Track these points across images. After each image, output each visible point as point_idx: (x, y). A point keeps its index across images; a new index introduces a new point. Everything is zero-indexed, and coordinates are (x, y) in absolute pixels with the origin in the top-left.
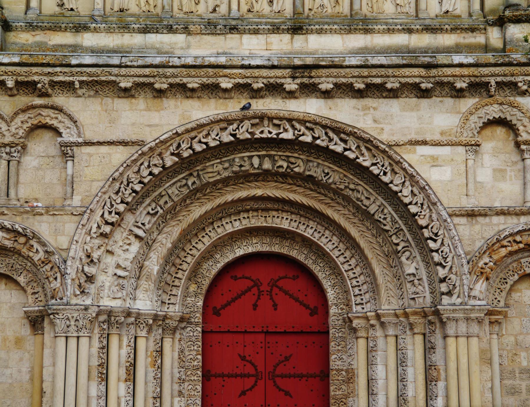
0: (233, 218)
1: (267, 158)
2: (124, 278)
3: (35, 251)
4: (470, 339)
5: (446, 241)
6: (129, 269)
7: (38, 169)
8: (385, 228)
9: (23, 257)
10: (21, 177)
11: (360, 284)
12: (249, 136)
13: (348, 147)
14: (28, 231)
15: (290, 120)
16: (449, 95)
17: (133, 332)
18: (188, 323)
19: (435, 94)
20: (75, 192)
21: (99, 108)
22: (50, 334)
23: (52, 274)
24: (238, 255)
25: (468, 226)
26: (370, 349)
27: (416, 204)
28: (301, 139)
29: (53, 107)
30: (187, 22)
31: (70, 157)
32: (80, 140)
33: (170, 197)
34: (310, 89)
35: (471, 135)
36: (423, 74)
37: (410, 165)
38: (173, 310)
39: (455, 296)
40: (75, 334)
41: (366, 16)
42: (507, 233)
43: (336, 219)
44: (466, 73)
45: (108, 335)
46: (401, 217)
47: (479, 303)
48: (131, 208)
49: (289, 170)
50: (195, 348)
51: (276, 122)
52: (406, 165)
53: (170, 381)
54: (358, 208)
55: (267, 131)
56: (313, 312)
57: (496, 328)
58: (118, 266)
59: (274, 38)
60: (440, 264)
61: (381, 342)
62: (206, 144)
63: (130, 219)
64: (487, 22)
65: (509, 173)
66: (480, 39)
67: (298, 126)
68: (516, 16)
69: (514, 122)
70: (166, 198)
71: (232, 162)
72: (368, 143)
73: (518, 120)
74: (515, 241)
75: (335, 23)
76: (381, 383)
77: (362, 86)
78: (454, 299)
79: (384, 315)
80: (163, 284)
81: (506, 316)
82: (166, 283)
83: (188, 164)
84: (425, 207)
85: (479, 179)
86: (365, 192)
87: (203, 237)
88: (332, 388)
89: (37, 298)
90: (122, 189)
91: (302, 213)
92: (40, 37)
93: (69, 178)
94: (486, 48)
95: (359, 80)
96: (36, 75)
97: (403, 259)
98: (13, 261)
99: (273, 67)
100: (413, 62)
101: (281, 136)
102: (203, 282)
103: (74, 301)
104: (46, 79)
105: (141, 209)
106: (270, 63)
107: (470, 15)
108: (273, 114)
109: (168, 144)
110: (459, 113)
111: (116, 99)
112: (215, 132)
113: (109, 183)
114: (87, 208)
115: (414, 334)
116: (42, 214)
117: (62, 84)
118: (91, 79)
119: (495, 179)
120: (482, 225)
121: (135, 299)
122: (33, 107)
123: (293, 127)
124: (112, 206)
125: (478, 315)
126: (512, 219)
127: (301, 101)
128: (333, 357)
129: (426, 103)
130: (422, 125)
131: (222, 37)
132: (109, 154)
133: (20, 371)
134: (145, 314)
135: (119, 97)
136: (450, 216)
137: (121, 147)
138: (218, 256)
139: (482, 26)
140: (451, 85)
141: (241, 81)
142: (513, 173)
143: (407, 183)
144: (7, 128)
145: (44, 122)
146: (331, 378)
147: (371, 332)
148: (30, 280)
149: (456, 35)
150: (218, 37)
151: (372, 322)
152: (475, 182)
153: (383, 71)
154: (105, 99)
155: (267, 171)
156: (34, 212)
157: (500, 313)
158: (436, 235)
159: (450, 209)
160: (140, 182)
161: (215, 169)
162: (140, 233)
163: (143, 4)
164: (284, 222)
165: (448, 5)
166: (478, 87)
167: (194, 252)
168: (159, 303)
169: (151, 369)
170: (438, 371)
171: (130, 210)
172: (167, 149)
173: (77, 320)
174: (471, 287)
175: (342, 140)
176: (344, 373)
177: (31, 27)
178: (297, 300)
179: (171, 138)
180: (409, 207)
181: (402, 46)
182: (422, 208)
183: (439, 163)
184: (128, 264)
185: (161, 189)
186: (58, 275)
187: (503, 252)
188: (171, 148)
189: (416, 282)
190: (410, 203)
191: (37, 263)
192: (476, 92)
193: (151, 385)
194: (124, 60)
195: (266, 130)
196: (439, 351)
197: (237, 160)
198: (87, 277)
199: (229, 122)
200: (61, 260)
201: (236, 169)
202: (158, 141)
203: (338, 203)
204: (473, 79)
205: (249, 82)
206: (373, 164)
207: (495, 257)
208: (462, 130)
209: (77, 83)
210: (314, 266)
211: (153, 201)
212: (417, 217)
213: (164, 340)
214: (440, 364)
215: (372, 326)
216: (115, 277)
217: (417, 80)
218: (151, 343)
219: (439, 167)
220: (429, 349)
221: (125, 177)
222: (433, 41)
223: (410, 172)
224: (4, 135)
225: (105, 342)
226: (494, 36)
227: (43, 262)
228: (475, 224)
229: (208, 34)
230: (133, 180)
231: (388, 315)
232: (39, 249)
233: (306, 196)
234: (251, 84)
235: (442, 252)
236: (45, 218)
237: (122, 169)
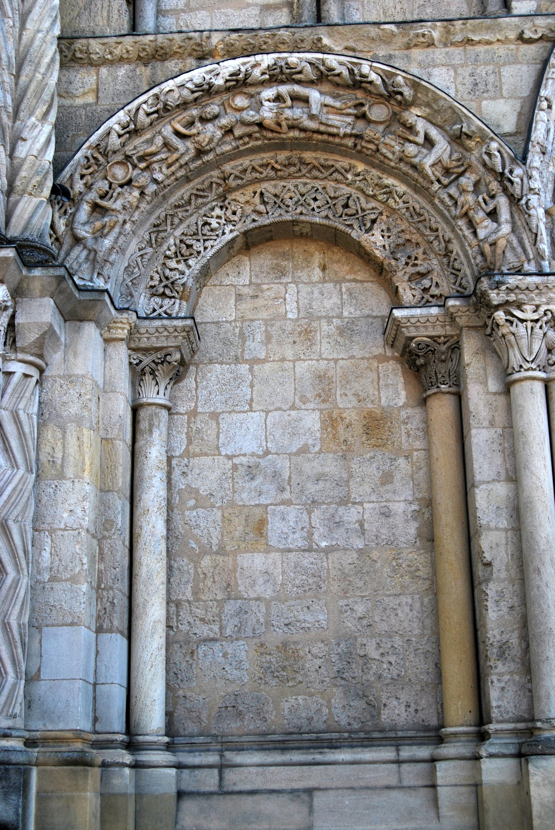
3: (420, 139)
14: (400, 79)
22: (485, 383)
23: (480, 199)
89: (425, 290)
98: (346, 190)
116: (431, 44)
133: (386, 514)
148: (400, 241)
186: (502, 202)
191: (429, 172)
227: (447, 172)
232: (434, 133)
236: (439, 54)
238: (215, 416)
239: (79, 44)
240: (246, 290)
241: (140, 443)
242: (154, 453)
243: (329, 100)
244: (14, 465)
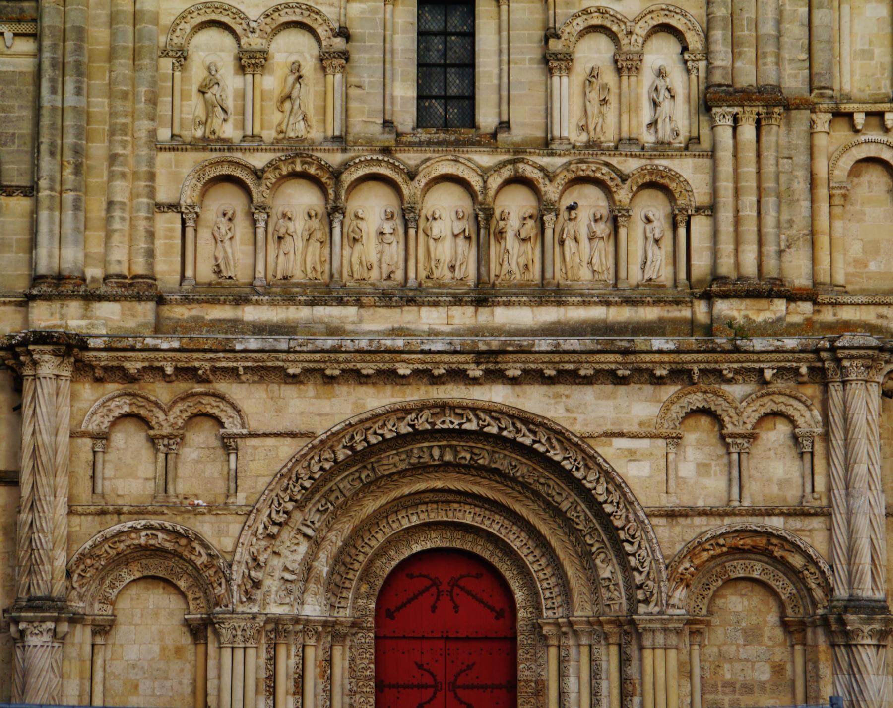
0: (410, 511)
1: (448, 449)
2: (291, 581)
3: (197, 554)
4: (668, 651)
5: (644, 544)
6: (297, 571)
7: (197, 461)
8: (578, 527)
9: (184, 560)
10: (179, 471)
11: (551, 586)
12: (429, 427)
13: (537, 439)
15: (474, 409)
17: (301, 640)
18: (359, 628)
20: (239, 489)
21: (264, 395)
24: (414, 551)
25: (667, 528)
26: (562, 659)
27: (612, 502)
28: (486, 430)
29: (214, 395)
30: (359, 293)
31: (234, 449)
32: (245, 431)
33: (341, 492)
34: (496, 376)
35: (672, 426)
37: (605, 460)
38: (343, 615)
39: (652, 605)
40: (242, 645)
41: (558, 284)
42: (709, 536)
43: (525, 515)
44: (667, 360)
45: (275, 644)
46: (596, 516)
47: (678, 612)
48: (300, 506)
49: (472, 462)
50: (368, 656)
51: (458, 411)
52: (601, 460)
53: (340, 694)
54: (548, 504)
55: (450, 422)
56: (499, 615)
57: (698, 639)
58: (286, 569)
59: (456, 311)
60: (637, 569)
61: (573, 651)
62: (382, 435)
63: (298, 516)
64: (692, 294)
65: (713, 468)
66: (686, 313)
67: (482, 415)
68: (724, 291)
69: (719, 412)
70: (338, 493)
71: (409, 454)
72: (560, 435)
74: (718, 544)
75: (525, 294)
76: (573, 696)
77: (553, 373)
78: (653, 608)
79: (576, 623)
80: (332, 586)
81: (708, 624)
82: (336, 584)
83: (362, 457)
84: (621, 506)
86: (556, 487)
87: (377, 532)
88: (520, 701)
90: (291, 486)
91: (486, 506)
92: (196, 311)
93: (232, 473)
94: (692, 326)
95: (550, 366)
96: (199, 361)
97: (598, 562)
99: (455, 352)
100: (608, 347)
101: (464, 427)
102: (376, 582)
103: (240, 609)
104: (207, 365)
105: (310, 505)
106: (453, 348)
107: (675, 286)
108: (456, 403)
109: (341, 436)
110: (659, 401)
111: (282, 386)
112: (392, 423)
113: (277, 479)
114: (254, 507)
115: (609, 644)
116: (204, 514)
117: (224, 370)
118: (256, 365)
119: (699, 474)
120: (683, 526)
121: (303, 604)
122: (193, 395)
123: (477, 416)
124: (280, 504)
125: (676, 625)
127: (487, 387)
128: (521, 667)
130: (619, 415)
131: (398, 310)
132: (276, 446)
133: (180, 683)
134: (314, 621)
135: (286, 383)
136: (648, 516)
137: (289, 439)
138: (392, 553)
139: (687, 299)
140: (651, 373)
141: (420, 367)
142: (718, 468)
143: (602, 480)
144: (164, 418)
145: (204, 411)
146: (519, 690)
147: (563, 640)
149: (659, 308)
150: (394, 310)
151: (564, 629)
152: (677, 477)
153: (576, 357)
154: (271, 385)
155: (448, 464)
156: (195, 510)
157: (701, 622)
158: (633, 537)
160: (310, 478)
161: (391, 461)
162: (309, 532)
163: (309, 270)
164: (468, 516)
165: (651, 272)
166: (680, 374)
167: (367, 549)
168: (329, 606)
169: (320, 681)
170: (634, 686)
171: (298, 507)
172: (339, 441)
173: (244, 630)
174: (670, 594)
175: (530, 431)
176: (533, 684)
177: (187, 300)
178: (480, 601)
179: (343, 430)
180: (604, 506)
181: (599, 320)
182: (618, 507)
184: (294, 566)
185: (332, 484)
186: (223, 580)
187: (705, 556)
188: (344, 440)
189: (612, 587)
190: (605, 502)
193: (320, 698)
194: (292, 344)
195: (448, 419)
196: (635, 663)
197: (415, 451)
198: (253, 582)
199: (407, 411)
200: (226, 564)
201: (414, 460)
202: (329, 433)
203: (527, 497)
204: (674, 366)
205: (429, 367)
206: (565, 458)
207: (697, 562)
209: (241, 369)
210: (500, 564)
211: (323, 496)
212: (612, 518)
213: (335, 647)
214: (636, 677)
215: (565, 633)
216: (282, 581)
217: (613, 367)
218: (320, 653)
220: (624, 661)
221: (294, 472)
222: (633, 315)
223: (605, 468)
224: (162, 426)
225: (273, 653)
226: (701, 310)
227: (206, 566)
229: (383, 306)
230: (302, 476)
231: (581, 622)
232: (202, 552)
233: (491, 488)
234: (431, 370)
235: (639, 556)
236: (208, 517)
237: (290, 464)
238: (121, 645)
239: (73, 508)
240: (134, 597)
241: (95, 658)
242: (99, 662)
243: (165, 537)
244: (56, 677)
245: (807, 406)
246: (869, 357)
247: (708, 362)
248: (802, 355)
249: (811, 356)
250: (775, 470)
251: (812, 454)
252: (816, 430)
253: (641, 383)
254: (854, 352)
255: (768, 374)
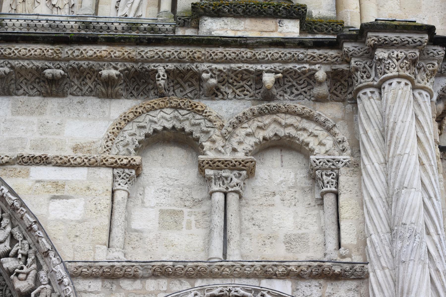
16: (94, 93)
19: (72, 90)
36: (49, 53)
37: (11, 191)
65: (186, 218)
69: (196, 134)
73: (203, 132)
84: (29, 261)
85: (135, 225)
119: (163, 226)
126: (181, 283)
129: (56, 105)
130: (44, 136)
136: (73, 276)
140: (94, 73)
142: (193, 218)
152: (128, 230)
159: (73, 264)
182: (25, 263)
183: (66, 193)
192: (138, 89)
204: (129, 65)
208: (110, 143)
219: (64, 200)
223: (10, 202)
228: (116, 292)
245: (329, 130)
246: (416, 45)
247: (180, 60)
248: (318, 52)
249: (332, 53)
250: (280, 218)
251: (337, 195)
252: (341, 158)
253: (83, 95)
254: (392, 36)
255: (268, 79)
